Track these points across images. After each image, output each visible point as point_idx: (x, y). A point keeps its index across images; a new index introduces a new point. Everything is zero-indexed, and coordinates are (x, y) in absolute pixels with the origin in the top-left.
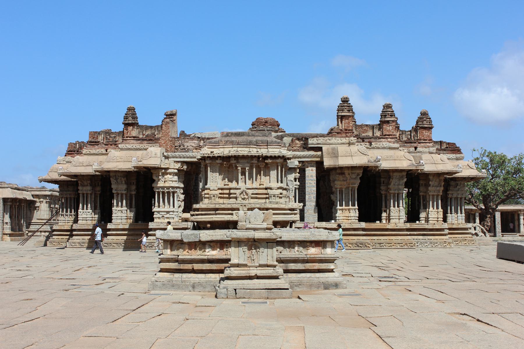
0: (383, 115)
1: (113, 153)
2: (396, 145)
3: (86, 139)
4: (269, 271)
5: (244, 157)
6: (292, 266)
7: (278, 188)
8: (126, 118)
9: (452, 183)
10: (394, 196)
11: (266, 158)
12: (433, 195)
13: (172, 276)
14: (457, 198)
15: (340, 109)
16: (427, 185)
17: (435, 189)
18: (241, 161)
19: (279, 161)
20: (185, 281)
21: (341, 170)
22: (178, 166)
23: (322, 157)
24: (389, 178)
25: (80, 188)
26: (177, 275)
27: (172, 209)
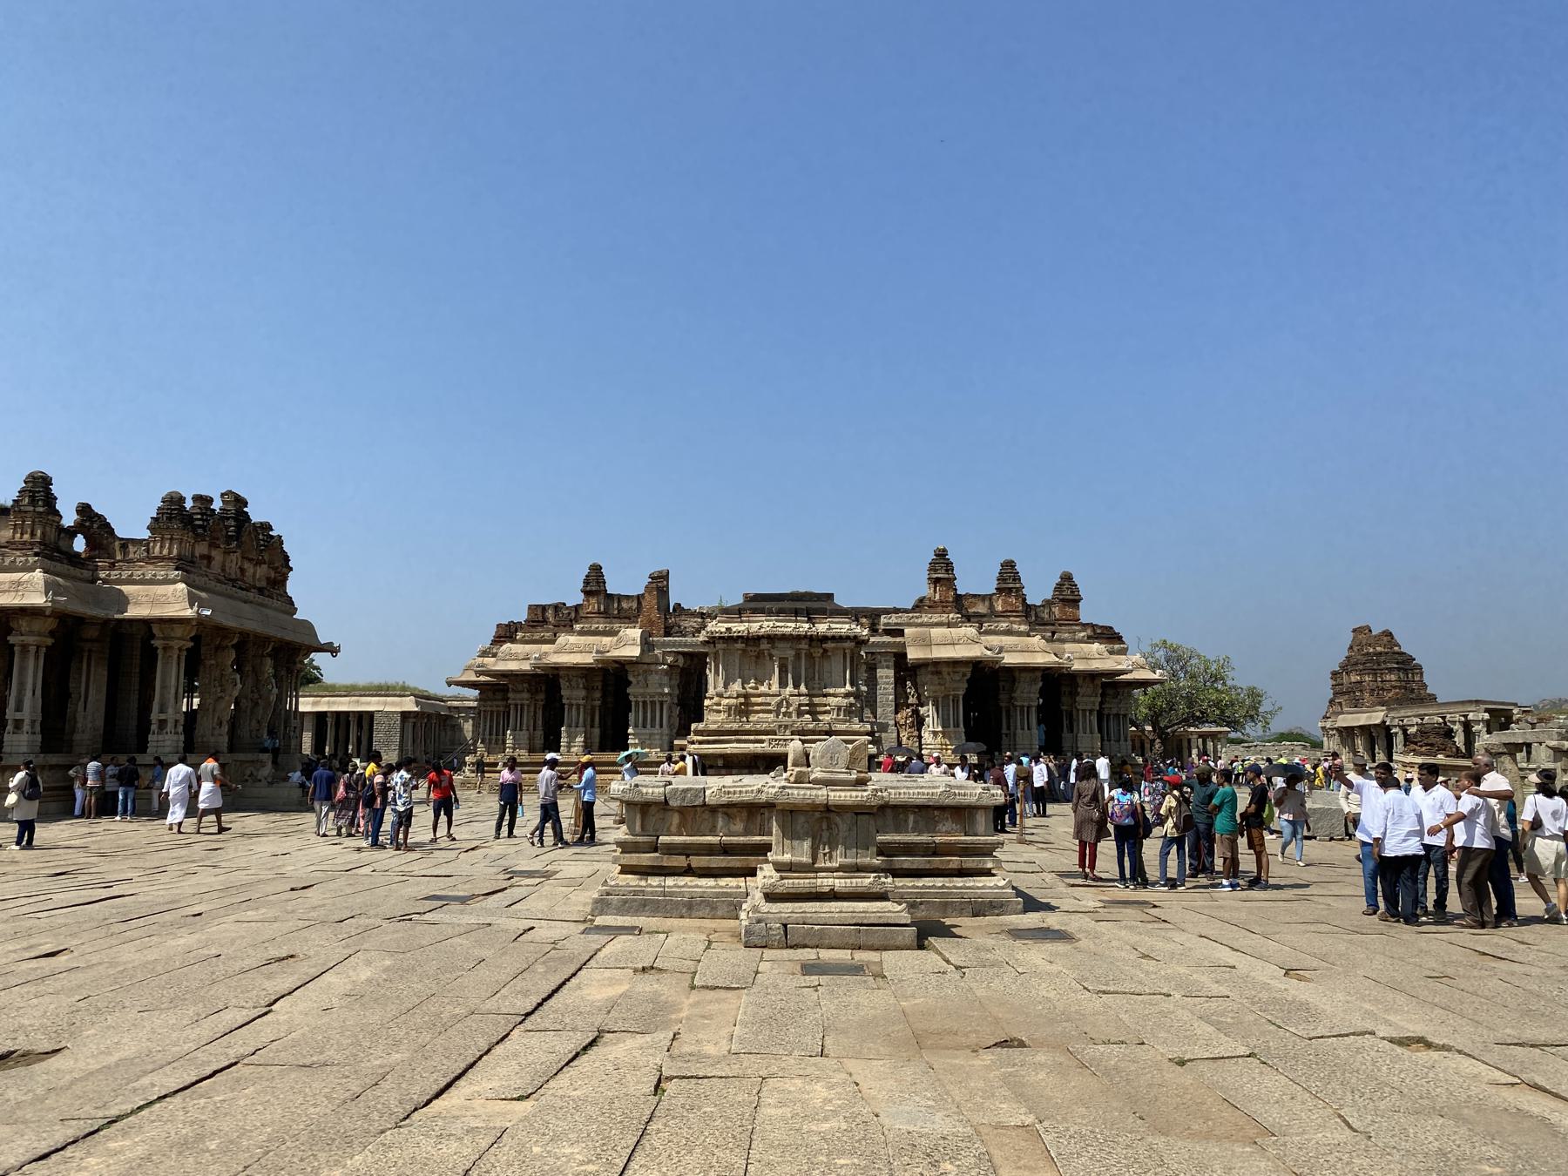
0: (1001, 579)
1: (563, 639)
2: (1023, 628)
3: (522, 616)
4: (866, 881)
5: (784, 638)
6: (905, 862)
7: (847, 695)
8: (586, 582)
9: (1110, 691)
11: (824, 639)
13: (643, 883)
14: (1117, 715)
15: (933, 568)
16: (1073, 694)
17: (1087, 700)
18: (780, 645)
19: (848, 644)
20: (672, 894)
21: (936, 666)
22: (670, 659)
24: (1014, 681)
25: (511, 695)
26: (654, 881)
27: (657, 730)
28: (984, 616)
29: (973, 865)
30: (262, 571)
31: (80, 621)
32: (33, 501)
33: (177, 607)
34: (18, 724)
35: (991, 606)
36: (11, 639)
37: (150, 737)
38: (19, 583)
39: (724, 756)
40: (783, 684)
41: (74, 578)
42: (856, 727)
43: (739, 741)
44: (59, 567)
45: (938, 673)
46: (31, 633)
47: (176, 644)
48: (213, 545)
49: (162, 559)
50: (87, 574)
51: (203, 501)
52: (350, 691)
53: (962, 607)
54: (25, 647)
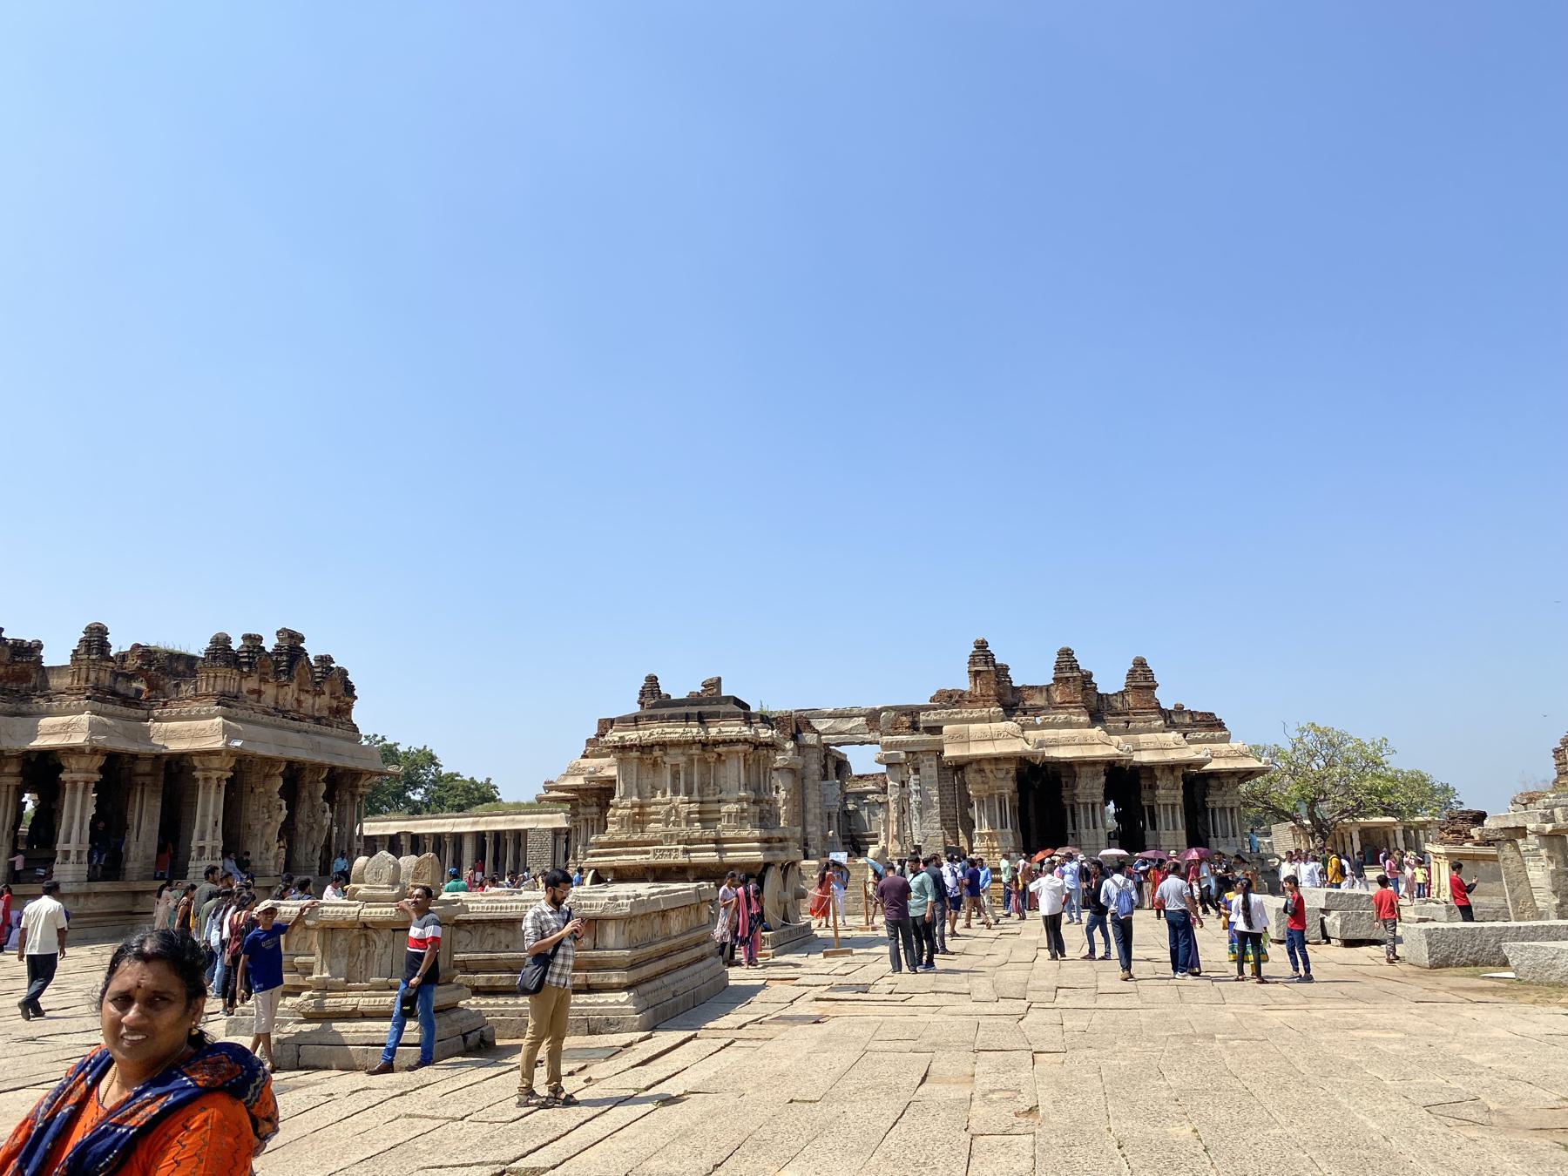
0: (1058, 668)
8: (642, 694)
9: (1213, 782)
10: (1086, 809)
11: (716, 743)
12: (1165, 805)
14: (1223, 809)
16: (1153, 787)
18: (671, 751)
23: (941, 743)
24: (1074, 776)
28: (1042, 708)
29: (599, 980)
30: (325, 700)
31: (135, 757)
32: (88, 652)
33: (213, 739)
34: (67, 854)
35: (1049, 698)
36: (63, 776)
37: (191, 864)
38: (68, 725)
39: (615, 869)
40: (676, 792)
41: (128, 718)
42: (744, 834)
43: (627, 853)
44: (110, 708)
45: (982, 771)
46: (79, 770)
47: (215, 775)
48: (263, 680)
49: (207, 696)
50: (141, 713)
51: (253, 641)
52: (519, 809)
53: (1011, 701)
54: (74, 783)
